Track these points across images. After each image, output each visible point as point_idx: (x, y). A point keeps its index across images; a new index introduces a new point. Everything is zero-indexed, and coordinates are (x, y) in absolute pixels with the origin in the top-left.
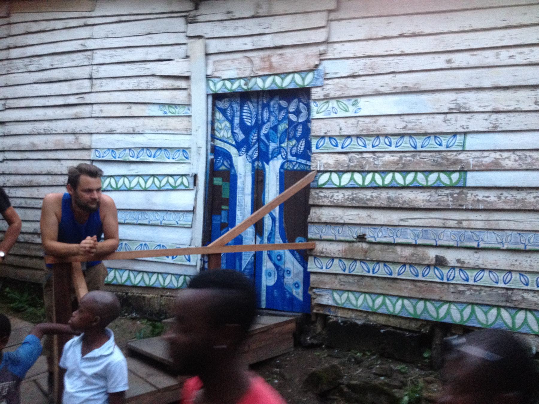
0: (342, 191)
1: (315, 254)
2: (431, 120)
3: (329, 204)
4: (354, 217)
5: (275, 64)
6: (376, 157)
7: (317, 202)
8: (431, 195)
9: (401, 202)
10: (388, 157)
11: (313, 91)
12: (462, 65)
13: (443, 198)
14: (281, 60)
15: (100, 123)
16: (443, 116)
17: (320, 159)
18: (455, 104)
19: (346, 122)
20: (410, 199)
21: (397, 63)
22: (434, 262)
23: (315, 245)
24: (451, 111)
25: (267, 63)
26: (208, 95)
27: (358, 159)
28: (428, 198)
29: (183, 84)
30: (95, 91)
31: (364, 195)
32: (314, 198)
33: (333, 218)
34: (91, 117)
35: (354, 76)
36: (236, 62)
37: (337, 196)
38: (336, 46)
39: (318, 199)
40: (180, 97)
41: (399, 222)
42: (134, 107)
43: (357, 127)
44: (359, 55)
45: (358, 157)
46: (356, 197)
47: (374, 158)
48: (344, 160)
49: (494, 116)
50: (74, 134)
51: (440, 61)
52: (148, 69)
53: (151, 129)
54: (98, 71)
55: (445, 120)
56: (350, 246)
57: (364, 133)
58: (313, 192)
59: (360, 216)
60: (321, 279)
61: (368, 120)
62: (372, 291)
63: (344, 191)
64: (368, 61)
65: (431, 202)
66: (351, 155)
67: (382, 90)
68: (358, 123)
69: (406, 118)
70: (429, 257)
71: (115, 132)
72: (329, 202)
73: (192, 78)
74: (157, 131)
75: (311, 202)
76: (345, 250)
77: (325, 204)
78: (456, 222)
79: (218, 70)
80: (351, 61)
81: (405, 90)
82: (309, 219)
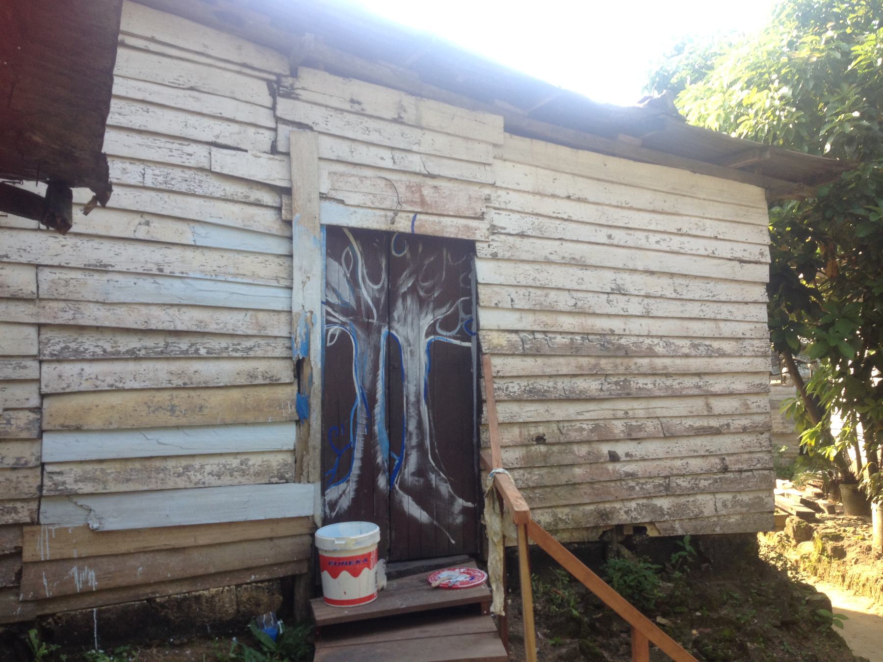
2: (597, 299)
3: (506, 398)
4: (532, 413)
8: (602, 384)
11: (478, 246)
12: (621, 243)
14: (437, 195)
15: (63, 246)
16: (606, 296)
17: (490, 338)
19: (517, 292)
22: (608, 458)
25: (417, 195)
27: (530, 340)
29: (268, 198)
33: (512, 417)
35: (522, 235)
36: (368, 182)
37: (513, 387)
38: (500, 192)
42: (156, 223)
44: (526, 211)
46: (533, 388)
47: (546, 340)
48: (517, 341)
49: (646, 301)
51: (601, 236)
52: (191, 155)
53: (202, 272)
56: (528, 452)
57: (538, 307)
61: (539, 292)
62: (554, 504)
66: (522, 335)
67: (553, 258)
69: (575, 294)
71: (110, 269)
73: (294, 191)
77: (502, 398)
78: (623, 412)
80: (518, 216)
81: (573, 262)
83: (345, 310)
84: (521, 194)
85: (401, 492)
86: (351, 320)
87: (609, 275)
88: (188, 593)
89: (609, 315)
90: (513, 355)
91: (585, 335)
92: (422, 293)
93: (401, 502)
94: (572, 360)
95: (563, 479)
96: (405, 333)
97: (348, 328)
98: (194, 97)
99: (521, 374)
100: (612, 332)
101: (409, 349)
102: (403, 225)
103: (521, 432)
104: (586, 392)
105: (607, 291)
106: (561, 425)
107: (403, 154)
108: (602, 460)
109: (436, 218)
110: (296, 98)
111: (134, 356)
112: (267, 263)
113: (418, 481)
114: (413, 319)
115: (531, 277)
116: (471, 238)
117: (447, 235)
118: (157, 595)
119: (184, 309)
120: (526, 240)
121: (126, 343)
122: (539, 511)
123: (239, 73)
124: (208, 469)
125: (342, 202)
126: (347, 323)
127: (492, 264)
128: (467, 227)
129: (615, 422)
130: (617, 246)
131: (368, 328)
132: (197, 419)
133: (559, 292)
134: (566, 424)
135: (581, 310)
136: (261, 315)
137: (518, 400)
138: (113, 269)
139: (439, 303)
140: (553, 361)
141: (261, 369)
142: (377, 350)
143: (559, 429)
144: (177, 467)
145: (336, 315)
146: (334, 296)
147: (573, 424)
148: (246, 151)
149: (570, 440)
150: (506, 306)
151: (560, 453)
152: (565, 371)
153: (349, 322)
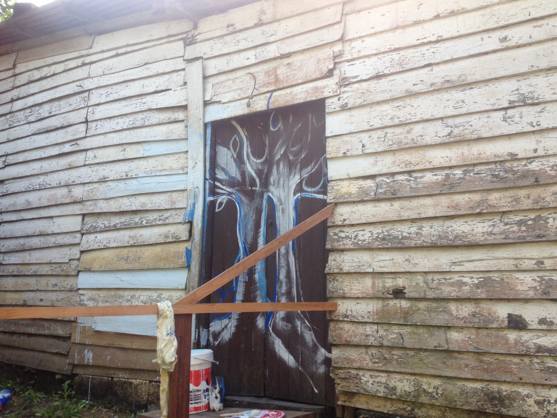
0: (368, 229)
1: (336, 318)
2: (486, 120)
3: (352, 247)
5: (281, 77)
6: (412, 179)
7: (336, 245)
8: (494, 226)
9: (451, 237)
10: (429, 177)
11: (328, 102)
13: (512, 227)
14: (288, 70)
16: (503, 112)
17: (339, 187)
18: (517, 95)
19: (370, 137)
20: (463, 232)
21: (434, 52)
23: (336, 305)
24: (512, 105)
26: (206, 125)
28: (490, 229)
29: (180, 115)
30: (89, 135)
31: (399, 231)
32: (333, 240)
33: (359, 266)
34: (85, 165)
35: (378, 77)
36: (238, 81)
37: (363, 235)
38: (354, 44)
39: (338, 241)
40: (178, 130)
41: (450, 267)
43: (384, 141)
44: (383, 50)
45: (388, 181)
46: (388, 235)
50: (67, 186)
52: (145, 103)
54: (93, 113)
55: (504, 117)
56: (384, 306)
57: (395, 147)
58: (331, 232)
59: (394, 261)
60: (346, 354)
61: (398, 130)
62: (417, 371)
63: (371, 228)
64: (395, 56)
65: (494, 234)
66: (378, 179)
67: (416, 89)
68: (385, 137)
69: (450, 122)
70: (498, 317)
71: (107, 179)
72: (351, 244)
74: (151, 173)
75: (328, 246)
76: (377, 311)
77: (347, 247)
79: (218, 93)
80: (375, 59)
81: (447, 85)
82: (327, 269)
83: (232, 183)
84: (379, 36)
85: (273, 334)
86: (237, 190)
87: (512, 85)
88: (128, 379)
89: (509, 136)
90: (362, 201)
91: (467, 166)
92: (291, 158)
93: (273, 343)
94: (444, 201)
95: (432, 343)
96: (278, 194)
97: (234, 196)
98: (147, 68)
99: (370, 221)
100: (514, 157)
101: (281, 207)
102: (260, 105)
103: (374, 284)
104: (466, 236)
105: (501, 107)
106: (430, 277)
107: (263, 48)
108: (495, 325)
109: (288, 91)
110: (195, 43)
111: (116, 229)
112: (179, 159)
113: (286, 326)
114: (284, 181)
115: (389, 117)
116: (319, 98)
117: (297, 102)
118: (115, 376)
119: (138, 197)
120: (384, 81)
121: (116, 220)
122: (398, 376)
123: (168, 42)
124: (142, 298)
125: (219, 102)
126: (233, 193)
127: (344, 116)
128: (316, 89)
129: (520, 276)
130: (518, 47)
131: (251, 195)
132: (137, 265)
133: (427, 125)
134: (437, 277)
135: (458, 138)
136: (174, 195)
137: (368, 249)
138: (109, 179)
139: (305, 164)
140: (415, 203)
141: (172, 232)
142: (259, 212)
143: (425, 282)
144: (128, 296)
145: (224, 188)
146: (223, 174)
147: (448, 277)
148: (171, 90)
149: (442, 296)
150: (355, 153)
151: (429, 310)
152: (430, 213)
153: (234, 191)
